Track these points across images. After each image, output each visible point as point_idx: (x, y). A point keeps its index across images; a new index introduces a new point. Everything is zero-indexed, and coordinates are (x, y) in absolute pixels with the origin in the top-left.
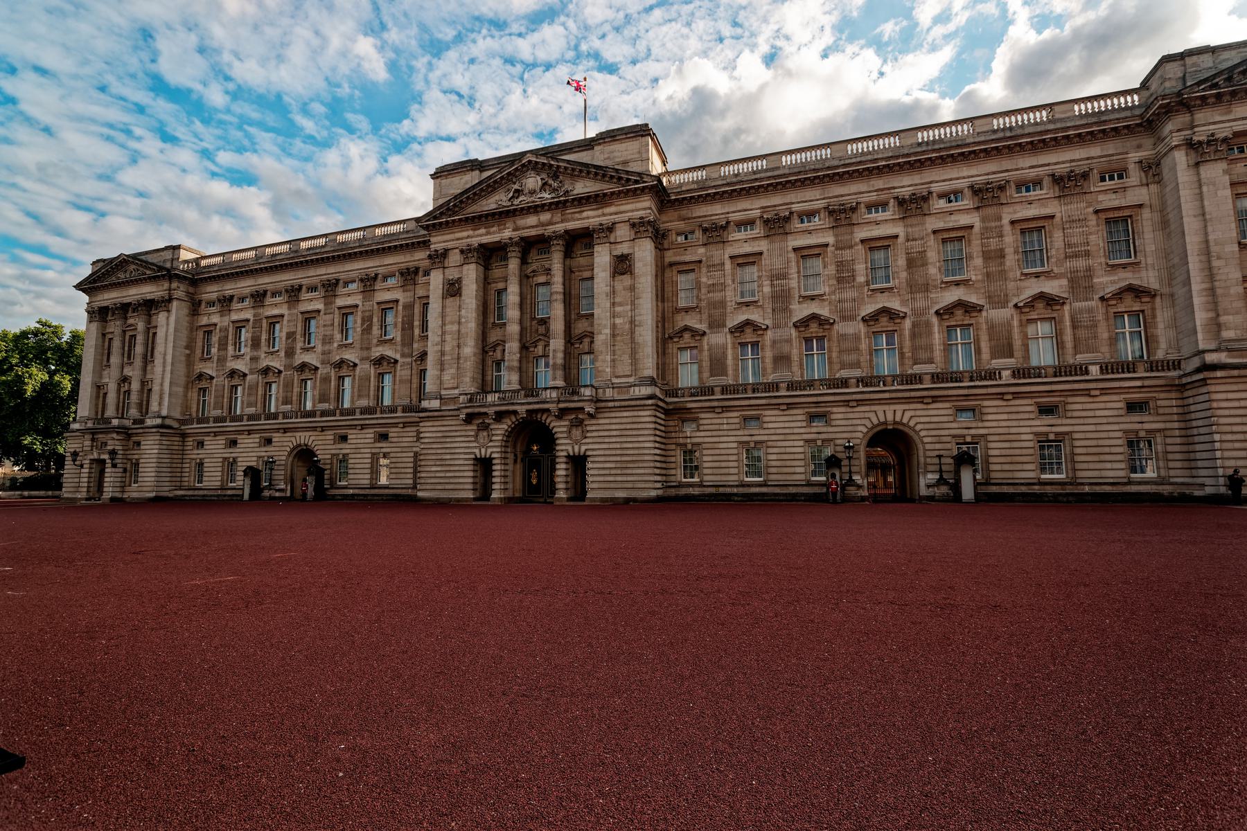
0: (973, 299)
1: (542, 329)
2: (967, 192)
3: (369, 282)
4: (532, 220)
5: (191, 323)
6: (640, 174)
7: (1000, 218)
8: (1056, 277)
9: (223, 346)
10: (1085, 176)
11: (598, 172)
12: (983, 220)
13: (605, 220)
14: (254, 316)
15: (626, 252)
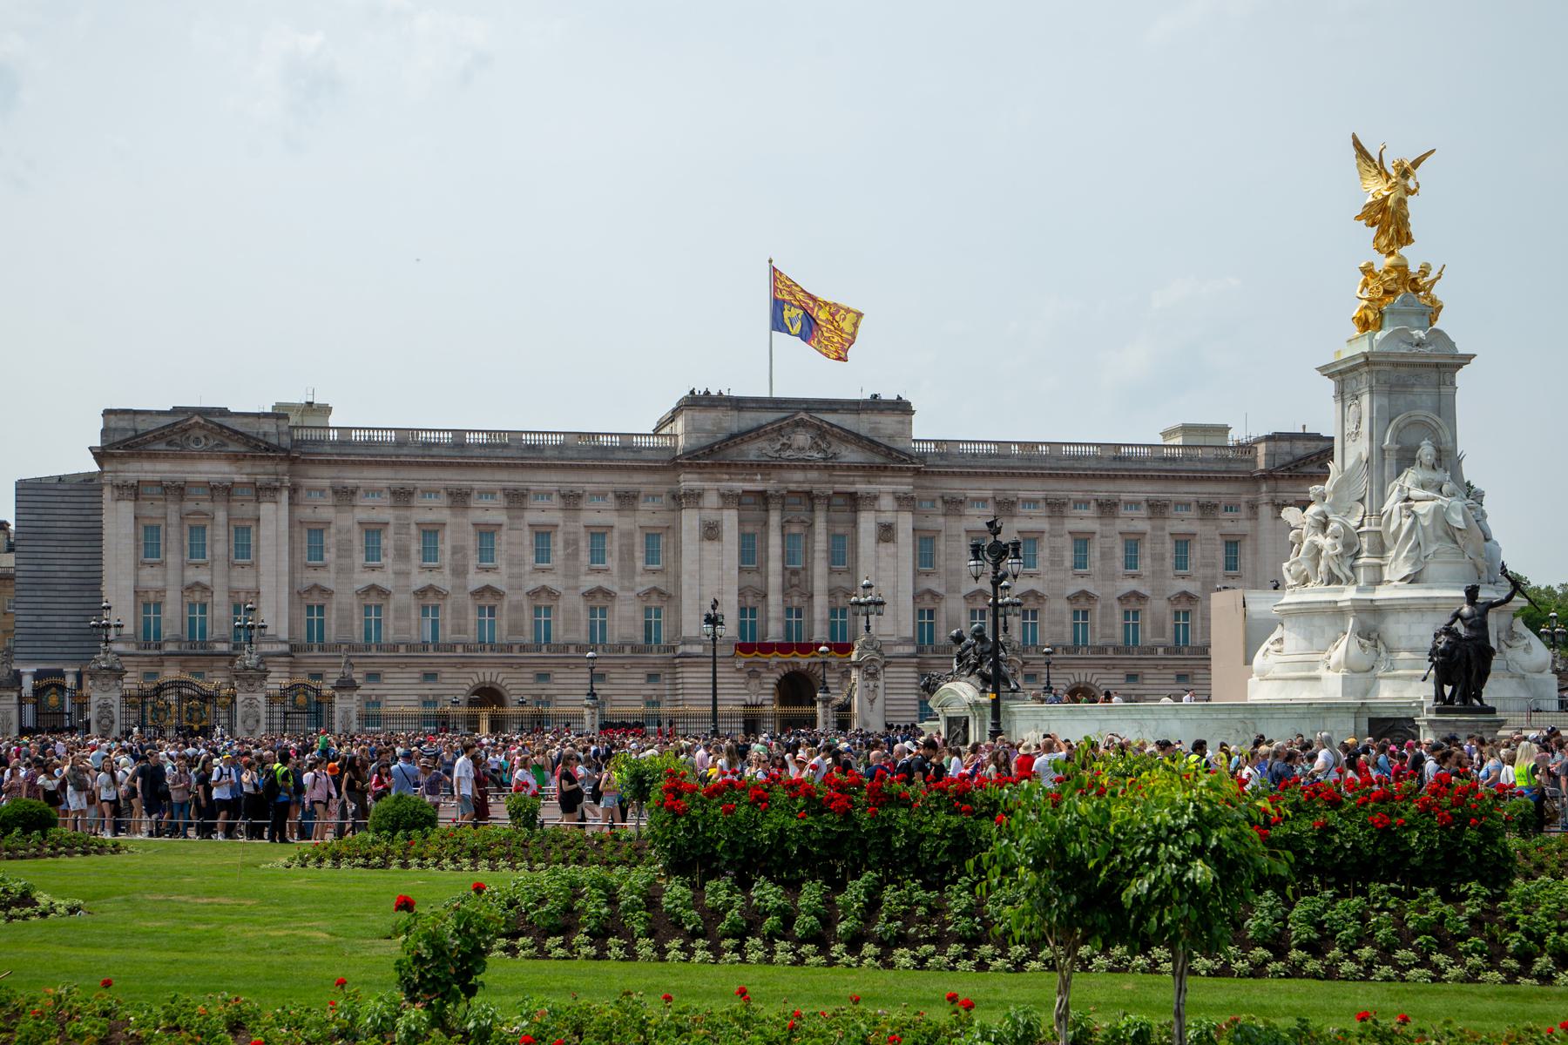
0: (1143, 590)
1: (795, 580)
2: (1144, 505)
3: (571, 500)
4: (798, 476)
5: (291, 513)
6: (911, 457)
7: (1163, 529)
8: (1194, 580)
9: (344, 550)
10: (1216, 506)
11: (870, 444)
12: (1153, 528)
13: (873, 488)
14: (397, 518)
15: (890, 520)
